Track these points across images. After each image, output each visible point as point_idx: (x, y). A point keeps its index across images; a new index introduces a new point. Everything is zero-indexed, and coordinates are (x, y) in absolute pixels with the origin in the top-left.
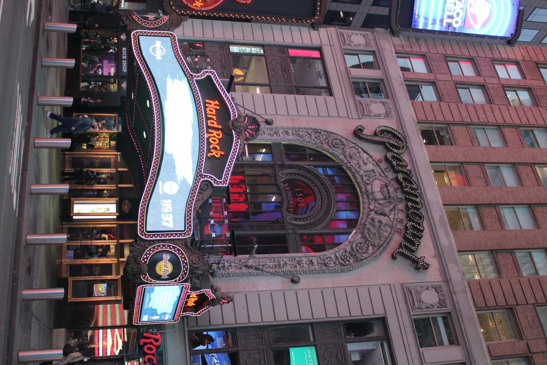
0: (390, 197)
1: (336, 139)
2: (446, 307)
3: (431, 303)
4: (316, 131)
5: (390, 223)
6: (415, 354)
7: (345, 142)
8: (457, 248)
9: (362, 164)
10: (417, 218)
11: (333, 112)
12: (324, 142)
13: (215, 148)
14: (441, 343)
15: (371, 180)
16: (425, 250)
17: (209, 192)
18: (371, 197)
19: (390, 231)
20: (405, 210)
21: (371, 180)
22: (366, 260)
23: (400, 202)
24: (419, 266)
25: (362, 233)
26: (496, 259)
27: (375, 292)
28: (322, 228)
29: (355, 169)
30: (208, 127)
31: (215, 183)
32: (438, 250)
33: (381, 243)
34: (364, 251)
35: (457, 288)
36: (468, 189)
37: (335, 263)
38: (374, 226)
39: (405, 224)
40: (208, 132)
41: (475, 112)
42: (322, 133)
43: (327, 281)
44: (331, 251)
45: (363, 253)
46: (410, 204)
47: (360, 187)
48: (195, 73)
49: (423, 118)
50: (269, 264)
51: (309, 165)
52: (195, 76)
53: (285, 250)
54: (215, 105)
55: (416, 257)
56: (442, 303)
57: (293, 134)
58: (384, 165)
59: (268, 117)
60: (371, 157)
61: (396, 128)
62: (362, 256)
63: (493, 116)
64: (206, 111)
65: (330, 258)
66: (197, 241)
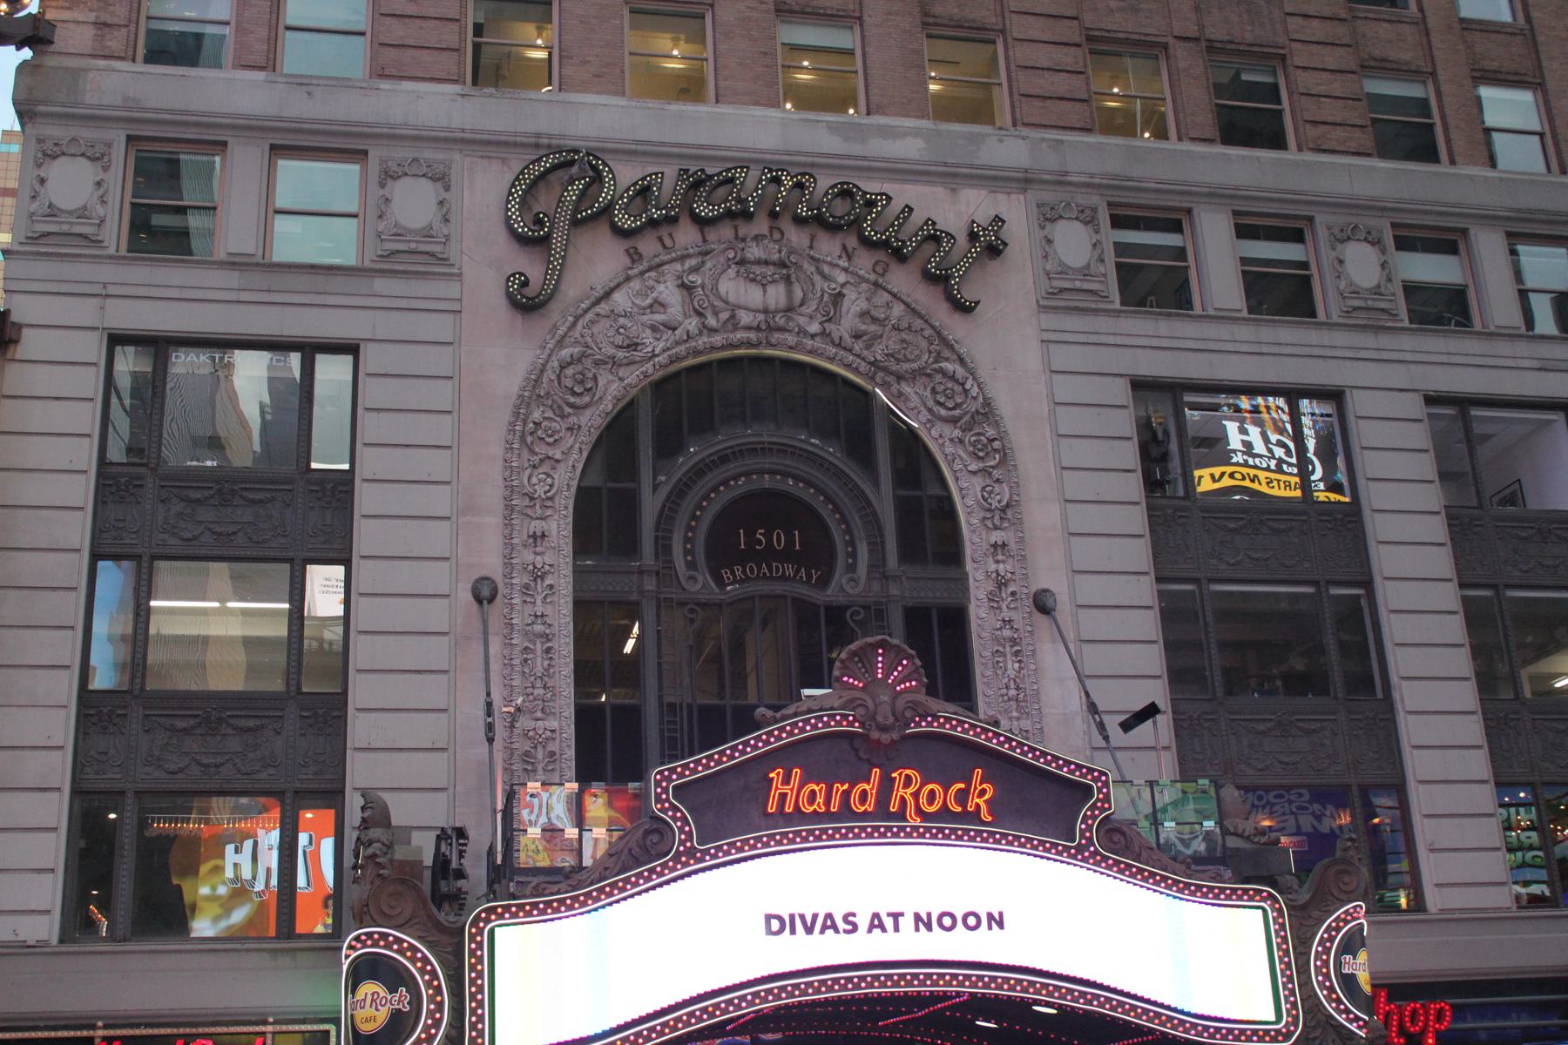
12: (573, 420)
13: (962, 797)
14: (1181, 253)
18: (781, 322)
19: (887, 296)
24: (989, 245)
25: (900, 378)
26: (945, 21)
29: (677, 343)
30: (882, 811)
34: (958, 388)
35: (1050, 161)
43: (1042, 515)
45: (966, 391)
51: (655, 487)
54: (786, 781)
56: (1090, 220)
58: (648, 246)
61: (517, 166)
65: (983, 489)
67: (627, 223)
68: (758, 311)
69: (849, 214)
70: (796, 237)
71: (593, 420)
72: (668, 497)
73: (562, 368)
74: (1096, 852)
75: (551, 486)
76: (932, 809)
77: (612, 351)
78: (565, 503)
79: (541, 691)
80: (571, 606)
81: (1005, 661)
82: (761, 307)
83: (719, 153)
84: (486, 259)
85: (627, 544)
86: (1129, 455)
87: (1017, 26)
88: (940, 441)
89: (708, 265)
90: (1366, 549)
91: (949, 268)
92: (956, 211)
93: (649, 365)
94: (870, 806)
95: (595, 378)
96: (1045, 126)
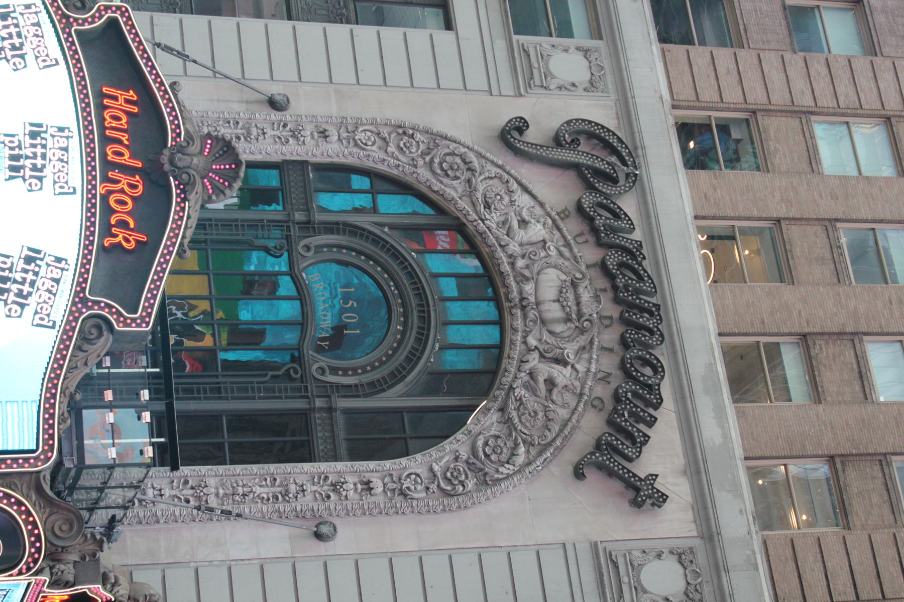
0: (580, 315)
1: (452, 154)
3: (665, 594)
4: (403, 131)
5: (577, 384)
7: (476, 164)
8: (745, 450)
9: (515, 224)
10: (648, 371)
11: (450, 76)
12: (420, 162)
13: (123, 224)
15: (536, 268)
16: (661, 457)
17: (106, 342)
18: (532, 314)
19: (573, 404)
20: (617, 348)
21: (536, 268)
22: (507, 483)
23: (607, 327)
24: (643, 495)
25: (502, 410)
26: (842, 479)
27: (525, 563)
28: (400, 397)
29: (497, 238)
30: (107, 165)
31: (118, 322)
32: (695, 455)
33: (549, 439)
34: (504, 457)
35: (734, 556)
36: (787, 292)
37: (428, 488)
38: (534, 392)
39: (614, 385)
40: (106, 179)
41: (828, 79)
42: (418, 136)
43: (405, 533)
44: (418, 456)
46: (632, 335)
47: (506, 286)
48: (78, 10)
49: (686, 94)
50: (258, 490)
52: (76, 20)
53: (302, 453)
55: (635, 475)
57: (339, 140)
58: (573, 226)
59: (274, 89)
60: (542, 205)
62: (497, 471)
63: (875, 90)
64: (101, 120)
65: (418, 475)
66: (69, 469)
68: (536, 298)
71: (424, 173)
72: (370, 232)
73: (461, 156)
74: (81, 313)
75: (366, 144)
82: (541, 299)
83: (665, 278)
88: (457, 445)
89: (567, 263)
93: (475, 217)
95: (457, 178)
96: (768, 561)
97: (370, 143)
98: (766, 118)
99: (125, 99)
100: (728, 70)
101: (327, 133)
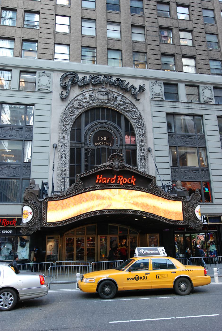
2: (161, 83)
6: (180, 104)
12: (70, 118)
13: (130, 181)
24: (142, 89)
37: (142, 129)
43: (150, 136)
45: (137, 114)
54: (100, 177)
65: (140, 131)
67: (81, 85)
69: (118, 84)
70: (109, 88)
71: (73, 118)
75: (66, 129)
76: (125, 183)
77: (77, 106)
78: (69, 133)
79: (64, 163)
80: (69, 149)
81: (142, 159)
84: (57, 90)
85: (79, 139)
86: (165, 125)
87: (149, 52)
90: (205, 141)
91: (136, 94)
92: (137, 84)
94: (114, 182)
96: (153, 69)
97: (66, 128)
98: (56, 41)
99: (99, 178)
100: (45, 46)
101: (64, 137)
